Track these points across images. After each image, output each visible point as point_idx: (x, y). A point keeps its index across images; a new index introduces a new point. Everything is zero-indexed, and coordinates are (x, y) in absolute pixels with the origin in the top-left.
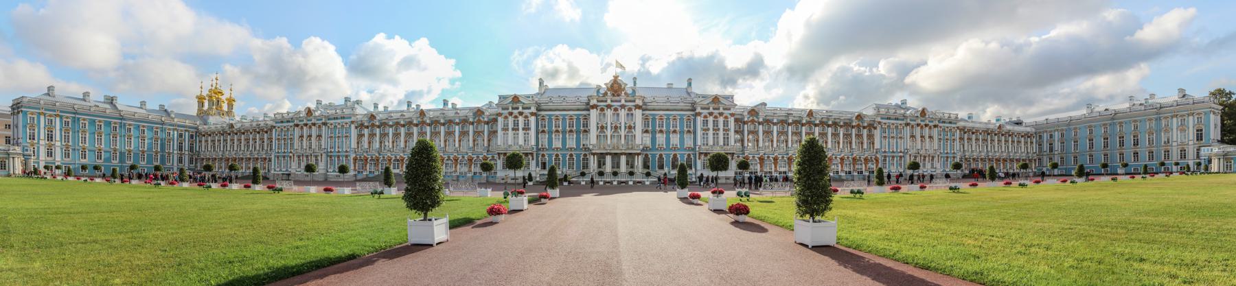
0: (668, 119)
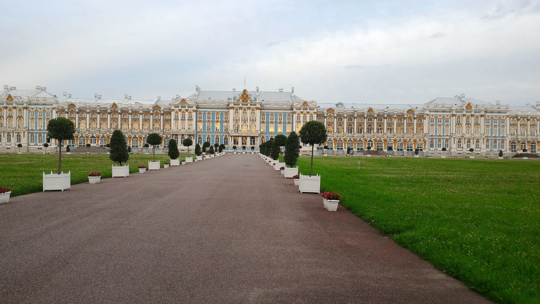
0: (276, 115)
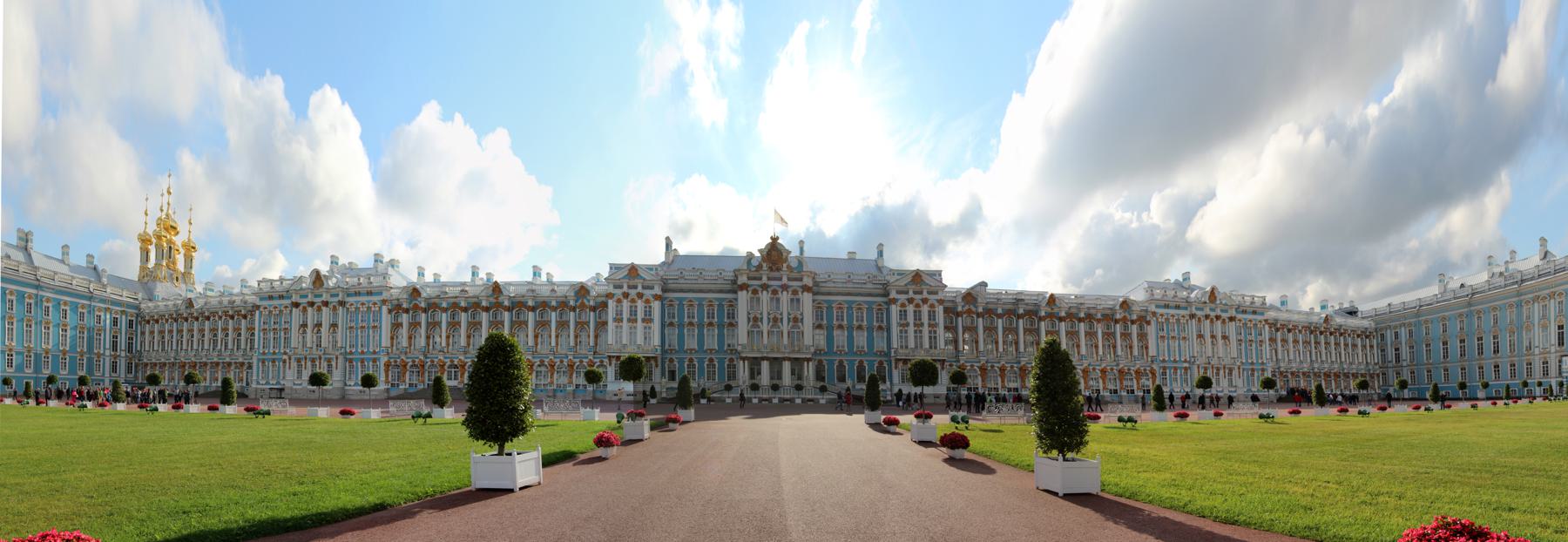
0: (850, 308)
